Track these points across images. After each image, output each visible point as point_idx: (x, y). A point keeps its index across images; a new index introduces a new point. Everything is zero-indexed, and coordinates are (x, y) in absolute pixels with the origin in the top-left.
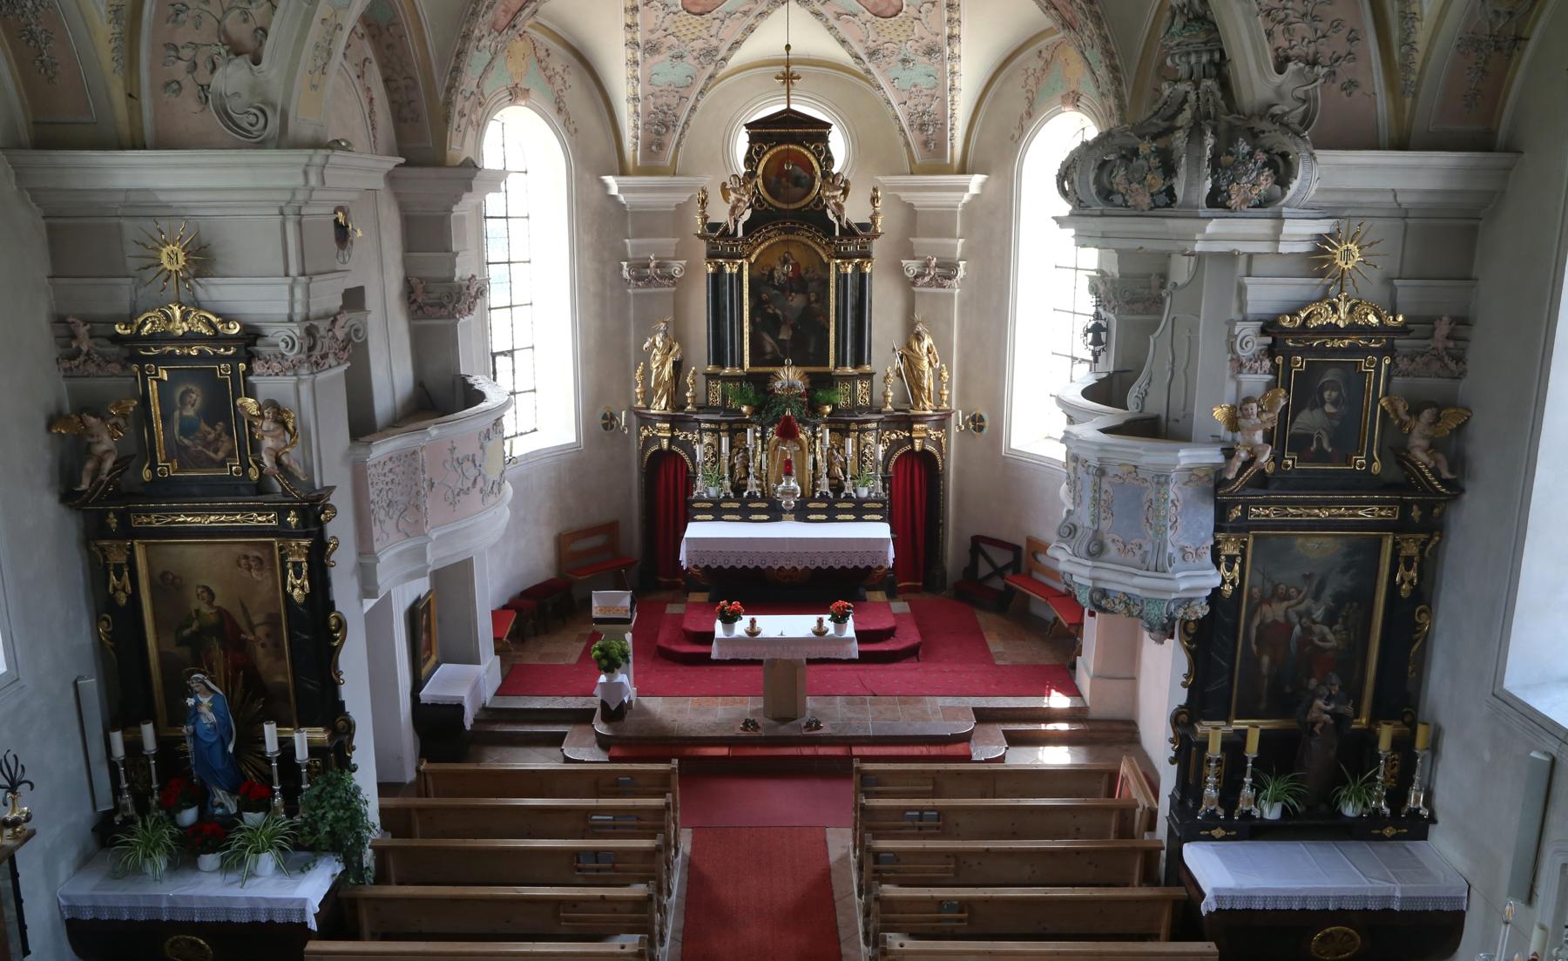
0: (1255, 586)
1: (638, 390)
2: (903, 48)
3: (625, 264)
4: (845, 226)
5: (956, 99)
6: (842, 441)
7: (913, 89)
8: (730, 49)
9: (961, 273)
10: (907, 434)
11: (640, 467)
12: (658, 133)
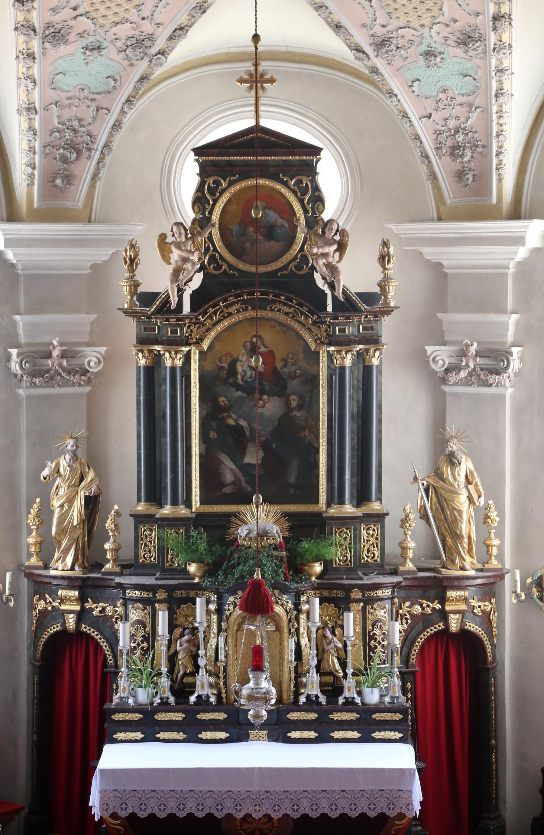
1: (31, 540)
2: (426, 35)
3: (14, 352)
4: (341, 297)
5: (505, 108)
6: (340, 616)
7: (442, 96)
8: (171, 38)
9: (515, 364)
10: (438, 606)
11: (32, 660)
12: (65, 160)
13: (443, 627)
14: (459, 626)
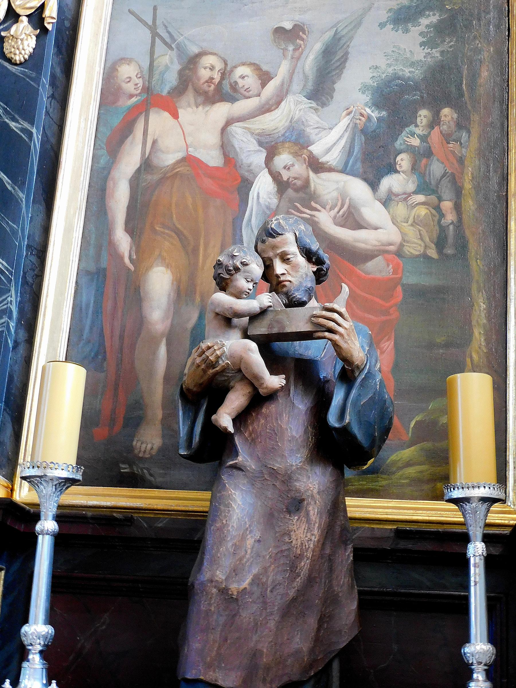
0: (123, 60)
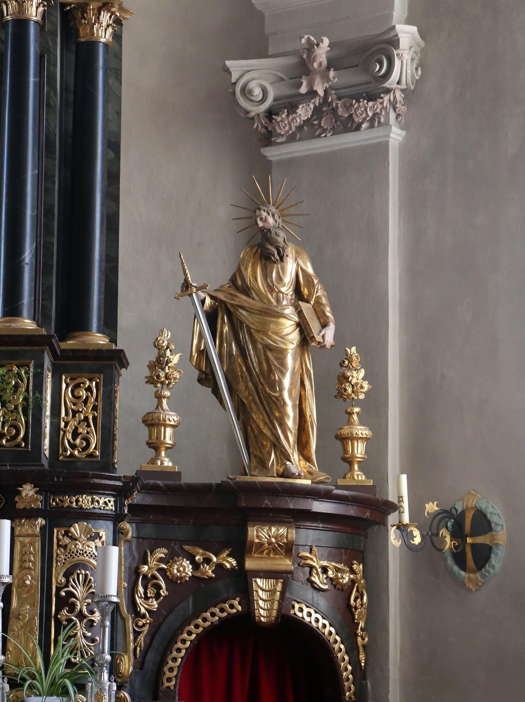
10: (230, 563)
13: (240, 608)
14: (276, 606)
